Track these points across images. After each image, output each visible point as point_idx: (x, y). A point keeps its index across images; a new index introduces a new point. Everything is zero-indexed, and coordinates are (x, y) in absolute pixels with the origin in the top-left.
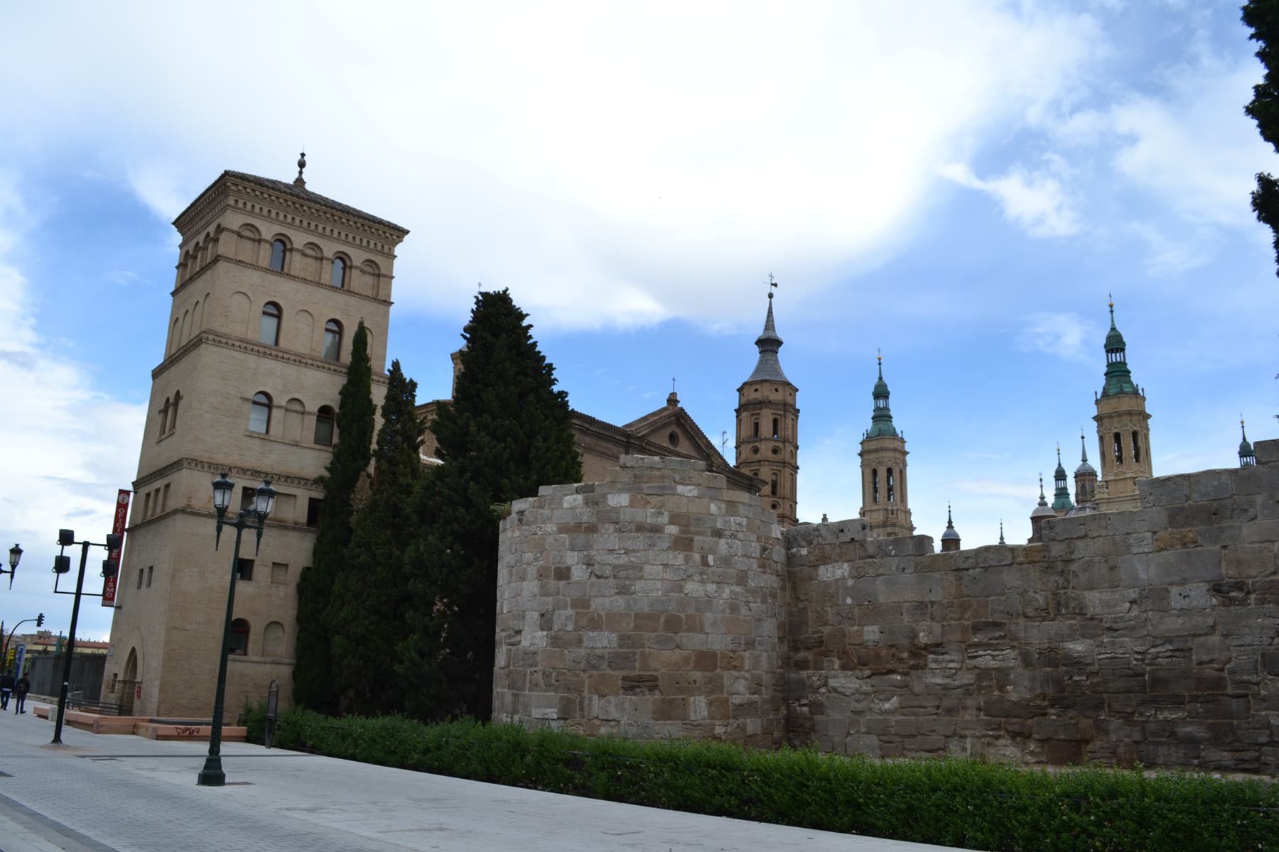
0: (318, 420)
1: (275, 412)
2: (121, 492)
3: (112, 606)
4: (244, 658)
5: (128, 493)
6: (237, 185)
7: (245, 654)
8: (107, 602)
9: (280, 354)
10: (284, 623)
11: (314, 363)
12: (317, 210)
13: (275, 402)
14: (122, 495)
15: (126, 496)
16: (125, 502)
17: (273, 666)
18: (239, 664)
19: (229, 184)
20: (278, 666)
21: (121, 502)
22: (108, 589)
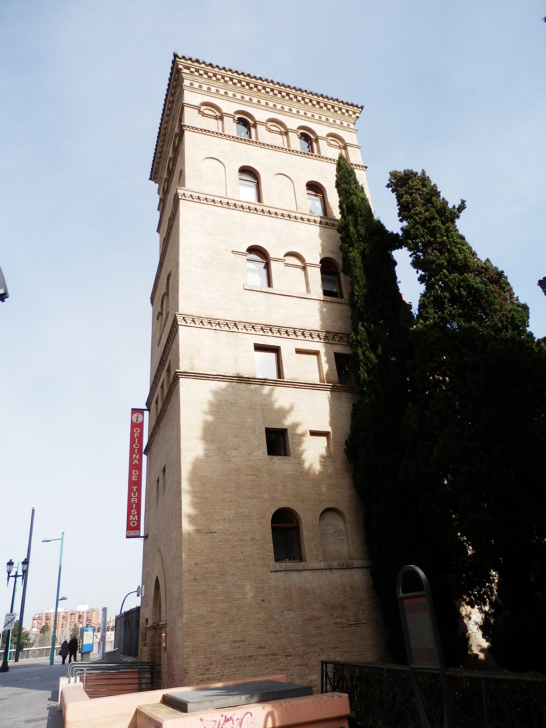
0: (322, 272)
1: (273, 264)
2: (134, 411)
3: (139, 537)
4: (301, 565)
5: (141, 411)
6: (188, 68)
7: (300, 558)
8: (132, 533)
9: (266, 209)
10: (342, 509)
11: (304, 216)
12: (272, 90)
13: (272, 255)
14: (135, 415)
15: (140, 415)
16: (140, 421)
17: (342, 572)
18: (294, 574)
19: (180, 66)
20: (349, 572)
21: (135, 421)
22: (131, 517)
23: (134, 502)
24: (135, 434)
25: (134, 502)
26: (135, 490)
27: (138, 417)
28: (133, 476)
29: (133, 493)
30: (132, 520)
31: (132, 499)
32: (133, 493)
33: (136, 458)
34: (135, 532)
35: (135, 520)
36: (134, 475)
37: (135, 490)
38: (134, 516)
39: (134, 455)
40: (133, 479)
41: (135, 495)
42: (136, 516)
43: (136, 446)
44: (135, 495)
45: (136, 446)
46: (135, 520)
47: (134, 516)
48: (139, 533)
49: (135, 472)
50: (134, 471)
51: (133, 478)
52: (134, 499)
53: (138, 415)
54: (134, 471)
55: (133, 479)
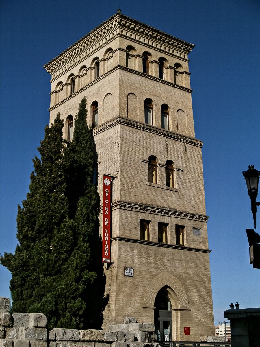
23: (107, 240)
24: (106, 193)
25: (107, 240)
26: (107, 232)
27: (107, 181)
28: (106, 222)
29: (106, 234)
30: (106, 252)
31: (106, 237)
32: (106, 234)
33: (107, 210)
34: (107, 260)
35: (107, 252)
36: (106, 222)
37: (107, 232)
38: (107, 249)
39: (106, 208)
40: (106, 225)
41: (107, 235)
42: (108, 249)
43: (107, 202)
44: (107, 235)
45: (107, 202)
46: (107, 252)
47: (107, 249)
48: (109, 260)
49: (107, 220)
50: (106, 219)
51: (106, 224)
52: (107, 238)
53: (107, 180)
54: (106, 219)
55: (106, 225)
